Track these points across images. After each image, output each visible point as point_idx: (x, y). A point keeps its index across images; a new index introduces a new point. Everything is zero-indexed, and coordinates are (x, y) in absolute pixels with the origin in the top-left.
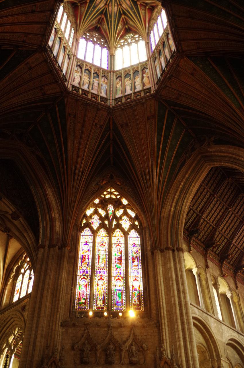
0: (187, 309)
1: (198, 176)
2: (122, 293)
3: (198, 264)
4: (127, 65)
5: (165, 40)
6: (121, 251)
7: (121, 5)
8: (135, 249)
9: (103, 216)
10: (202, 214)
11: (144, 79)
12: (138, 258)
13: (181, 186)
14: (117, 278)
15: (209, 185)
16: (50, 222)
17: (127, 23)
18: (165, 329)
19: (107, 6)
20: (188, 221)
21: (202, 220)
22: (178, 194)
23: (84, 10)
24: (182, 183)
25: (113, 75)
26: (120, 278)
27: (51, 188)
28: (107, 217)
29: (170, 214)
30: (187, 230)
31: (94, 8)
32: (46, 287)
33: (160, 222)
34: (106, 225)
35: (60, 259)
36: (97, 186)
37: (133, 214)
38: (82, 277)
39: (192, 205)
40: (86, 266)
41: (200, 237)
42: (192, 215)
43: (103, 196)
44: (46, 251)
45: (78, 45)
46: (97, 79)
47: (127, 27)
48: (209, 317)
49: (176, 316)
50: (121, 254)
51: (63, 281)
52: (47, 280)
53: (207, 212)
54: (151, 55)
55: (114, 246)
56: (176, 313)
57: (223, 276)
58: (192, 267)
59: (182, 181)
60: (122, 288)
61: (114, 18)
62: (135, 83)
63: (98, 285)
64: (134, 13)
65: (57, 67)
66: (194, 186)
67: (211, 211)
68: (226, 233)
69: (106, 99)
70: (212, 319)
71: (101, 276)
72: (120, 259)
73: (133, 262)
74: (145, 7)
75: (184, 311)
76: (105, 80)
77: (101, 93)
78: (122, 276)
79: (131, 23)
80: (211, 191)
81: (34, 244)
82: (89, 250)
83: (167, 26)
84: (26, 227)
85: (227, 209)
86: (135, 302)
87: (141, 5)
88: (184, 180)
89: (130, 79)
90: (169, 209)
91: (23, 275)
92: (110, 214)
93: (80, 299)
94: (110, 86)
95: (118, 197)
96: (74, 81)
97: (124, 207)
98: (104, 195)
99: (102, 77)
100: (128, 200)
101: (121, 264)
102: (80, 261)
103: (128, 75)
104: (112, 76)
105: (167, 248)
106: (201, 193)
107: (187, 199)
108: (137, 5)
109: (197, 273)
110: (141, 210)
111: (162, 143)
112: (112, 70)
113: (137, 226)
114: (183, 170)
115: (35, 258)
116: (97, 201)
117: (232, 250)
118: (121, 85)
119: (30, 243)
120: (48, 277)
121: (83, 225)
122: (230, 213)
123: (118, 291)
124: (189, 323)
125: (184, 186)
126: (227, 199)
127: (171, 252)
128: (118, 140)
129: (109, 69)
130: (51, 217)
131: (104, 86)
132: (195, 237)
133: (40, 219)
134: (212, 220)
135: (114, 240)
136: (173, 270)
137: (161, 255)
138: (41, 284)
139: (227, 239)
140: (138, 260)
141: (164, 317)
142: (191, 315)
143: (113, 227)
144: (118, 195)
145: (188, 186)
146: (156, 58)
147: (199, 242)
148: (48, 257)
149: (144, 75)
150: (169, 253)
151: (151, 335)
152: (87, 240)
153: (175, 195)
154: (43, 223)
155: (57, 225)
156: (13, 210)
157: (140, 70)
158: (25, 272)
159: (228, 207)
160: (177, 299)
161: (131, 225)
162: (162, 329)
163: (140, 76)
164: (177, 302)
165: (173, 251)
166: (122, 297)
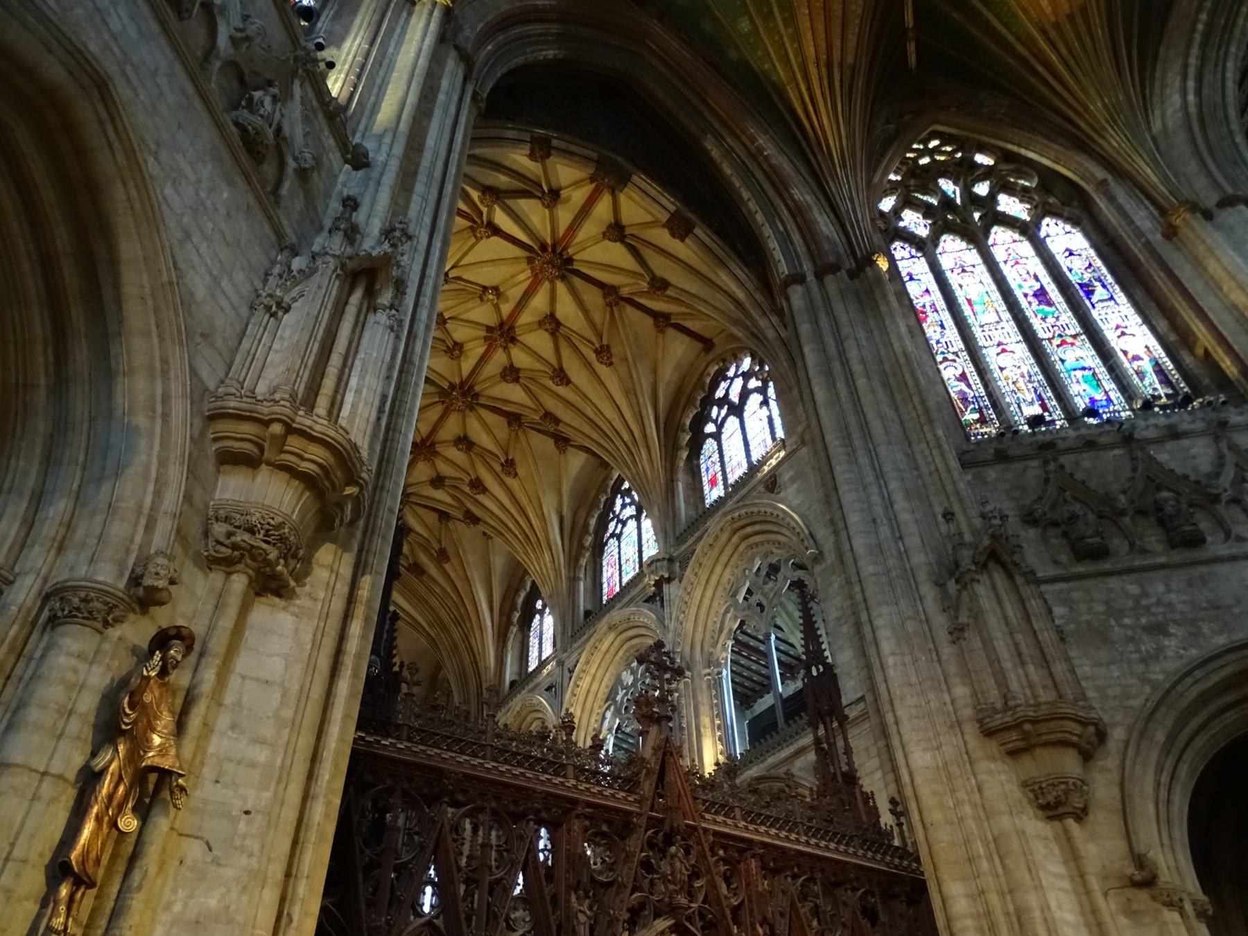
14: (1057, 341)
22: (1195, 51)
24: (1204, 16)
26: (1069, 340)
27: (766, 132)
36: (892, 126)
40: (939, 329)
52: (853, 354)
73: (1090, 293)
81: (758, 297)
82: (927, 291)
84: (720, 253)
86: (1155, 389)
91: (717, 436)
130: (791, 204)
135: (999, 254)
138: (837, 367)
145: (1227, 19)
154: (773, 225)
156: (672, 208)
158: (720, 427)
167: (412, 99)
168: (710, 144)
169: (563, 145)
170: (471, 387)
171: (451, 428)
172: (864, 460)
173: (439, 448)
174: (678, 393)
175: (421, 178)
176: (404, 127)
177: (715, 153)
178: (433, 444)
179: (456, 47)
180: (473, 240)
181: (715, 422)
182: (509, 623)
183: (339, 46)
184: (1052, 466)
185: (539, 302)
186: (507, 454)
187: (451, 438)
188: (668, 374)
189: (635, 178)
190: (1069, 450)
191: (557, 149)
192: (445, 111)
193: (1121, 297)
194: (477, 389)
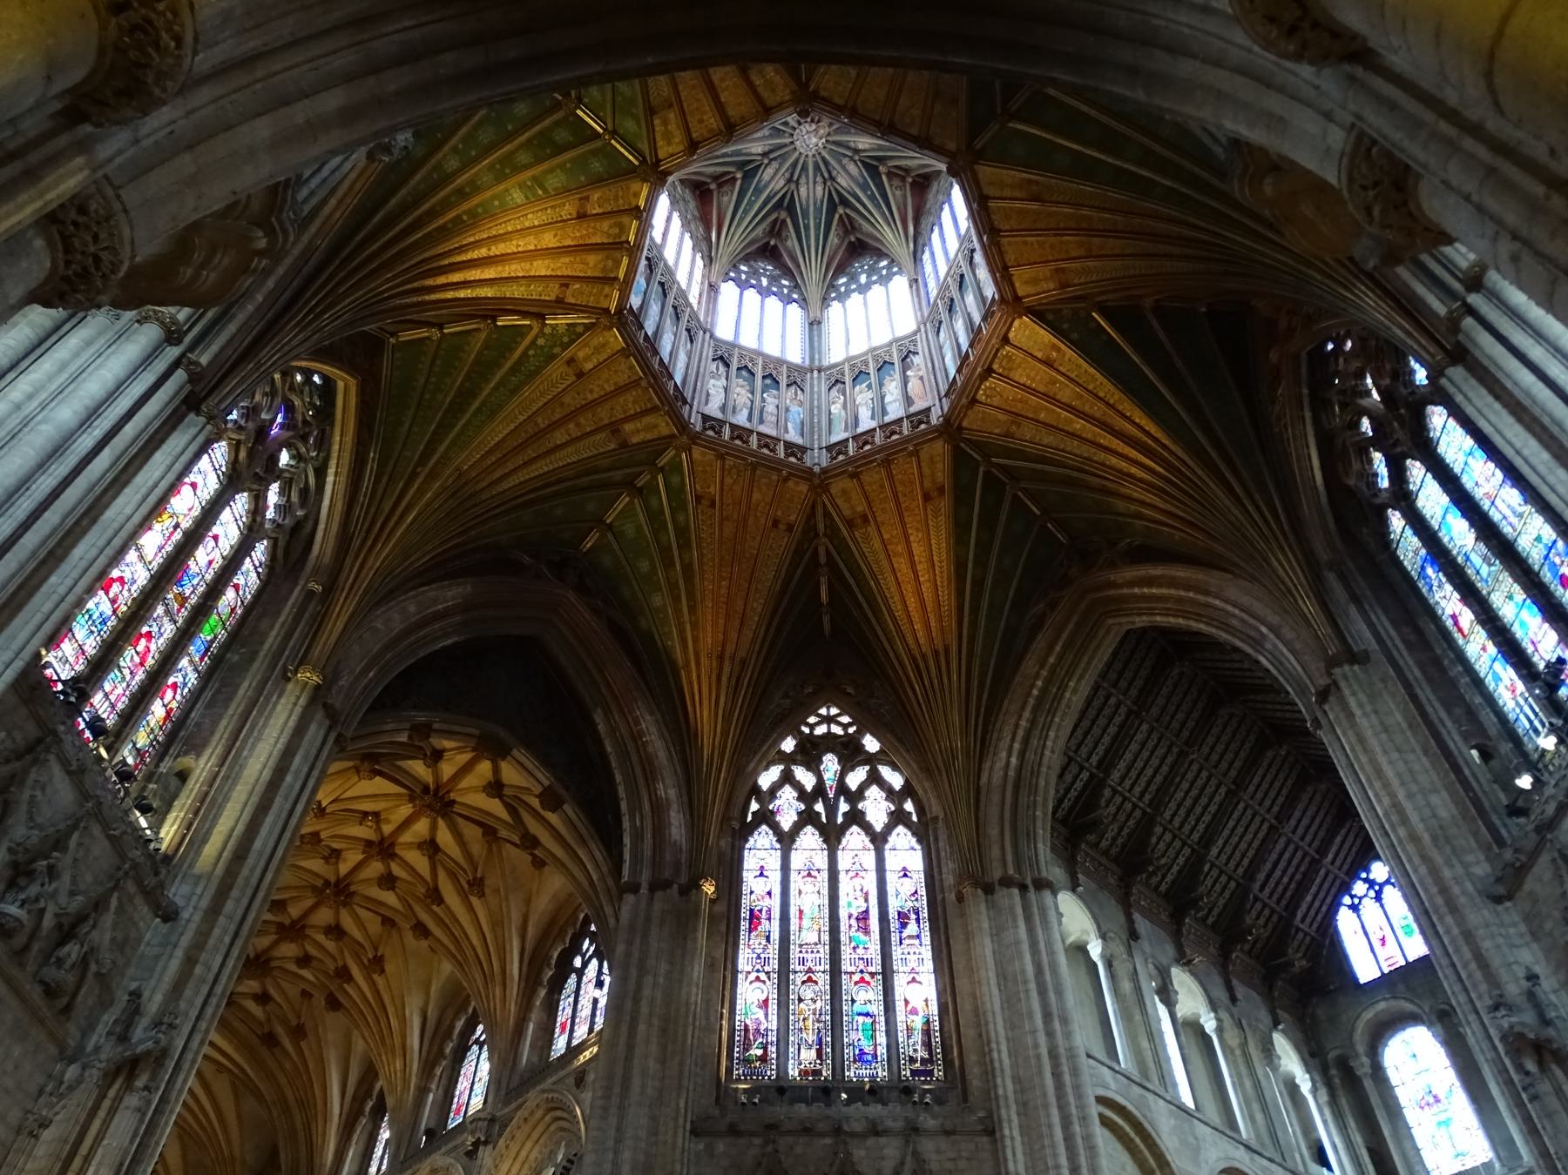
0: (1075, 1072)
1: (1085, 659)
2: (874, 1022)
3: (1104, 929)
4: (859, 347)
5: (965, 269)
6: (867, 894)
7: (833, 179)
8: (907, 886)
9: (809, 788)
10: (1107, 773)
11: (910, 385)
12: (917, 913)
13: (1035, 692)
14: (856, 977)
15: (1123, 684)
16: (653, 812)
17: (853, 228)
18: (1012, 1138)
19: (793, 186)
20: (1065, 796)
21: (1107, 793)
22: (1027, 714)
23: (730, 202)
24: (1039, 683)
25: (819, 378)
26: (867, 977)
27: (652, 713)
28: (820, 790)
29: (1006, 775)
30: (1064, 822)
31: (758, 191)
32: (644, 1010)
33: (977, 801)
34: (818, 814)
35: (683, 921)
36: (788, 701)
37: (896, 780)
38: (753, 976)
39: (1073, 748)
40: (764, 942)
41: (1104, 844)
42: (1076, 777)
43: (806, 730)
44: (643, 905)
45: (715, 300)
46: (775, 392)
47: (853, 239)
48: (1150, 1096)
49: (1045, 1095)
50: (866, 900)
51: (694, 990)
52: (646, 992)
53: (1122, 765)
54: (926, 314)
55: (842, 877)
56: (1043, 1086)
57: (1184, 961)
58: (1084, 937)
59: (1037, 676)
60: (872, 1009)
61: (815, 219)
62: (883, 398)
63: (800, 1000)
64: (872, 198)
65: (656, 367)
66: (1075, 691)
67: (1135, 761)
68: (1187, 828)
69: (803, 449)
70: (1161, 1102)
71: (810, 970)
72: (863, 917)
73: (904, 925)
74: (903, 179)
75: (1067, 1078)
76: (796, 394)
77: (787, 431)
78: (872, 969)
79: (866, 226)
80: (1128, 703)
82: (769, 893)
83: (969, 228)
84: (584, 832)
85: (1182, 754)
86: (915, 1051)
87: (890, 175)
88: (1044, 673)
89: (869, 387)
90: (1003, 760)
91: (580, 973)
92: (828, 783)
93: (747, 1046)
94: (812, 410)
95: (851, 730)
96: (707, 403)
97: (871, 760)
98: (807, 725)
99: (788, 385)
100: (879, 740)
101: (866, 931)
102: (744, 925)
103: (862, 376)
104: (816, 382)
105: (1006, 882)
106: (1100, 711)
107: (1058, 730)
108: (879, 175)
109: (1103, 956)
110: (921, 769)
111: (970, 565)
112: (817, 363)
113: (910, 813)
114: (1040, 642)
115: (612, 921)
116: (788, 745)
117: (1209, 882)
118: (845, 406)
119: (595, 877)
120: (649, 980)
121: (749, 818)
122: (1195, 767)
123: (861, 1019)
124: (1084, 1119)
125: (1044, 691)
126: (1183, 724)
127: (1016, 891)
128: (842, 565)
129: (807, 362)
130: (654, 798)
131: (797, 413)
132: (1087, 843)
133: (624, 806)
134: (1137, 790)
135: (844, 861)
136: (1025, 947)
137: (987, 901)
138: (629, 1004)
139: (1190, 846)
140: (918, 920)
141: (1006, 1098)
142: (1091, 1093)
143: (840, 820)
144: (850, 725)
145: (1058, 689)
146: (940, 322)
147: (1104, 860)
148: (648, 919)
149: (909, 373)
150: (1011, 896)
151: (968, 1159)
152: (762, 863)
153: (1020, 716)
155: (673, 821)
156: (546, 783)
157: (896, 360)
158: (585, 964)
159: (1186, 749)
160: (1042, 1039)
161: (891, 814)
162: (1003, 1137)
163: (897, 376)
164: (1044, 1051)
165: (1023, 888)
166: (873, 1037)
167: (240, 828)
168: (598, 717)
169: (445, 727)
170: (348, 885)
171: (324, 916)
172: (613, 1121)
173: (308, 932)
174: (552, 921)
175: (235, 893)
176: (220, 871)
177: (601, 728)
178: (304, 927)
179: (325, 706)
180: (356, 778)
181: (583, 956)
182: (360, 1112)
183: (198, 756)
184: (770, 1149)
185: (421, 827)
186: (376, 949)
187: (323, 924)
188: (543, 904)
189: (515, 752)
190: (789, 1132)
191: (437, 731)
192: (286, 799)
193: (926, 939)
194: (353, 888)
